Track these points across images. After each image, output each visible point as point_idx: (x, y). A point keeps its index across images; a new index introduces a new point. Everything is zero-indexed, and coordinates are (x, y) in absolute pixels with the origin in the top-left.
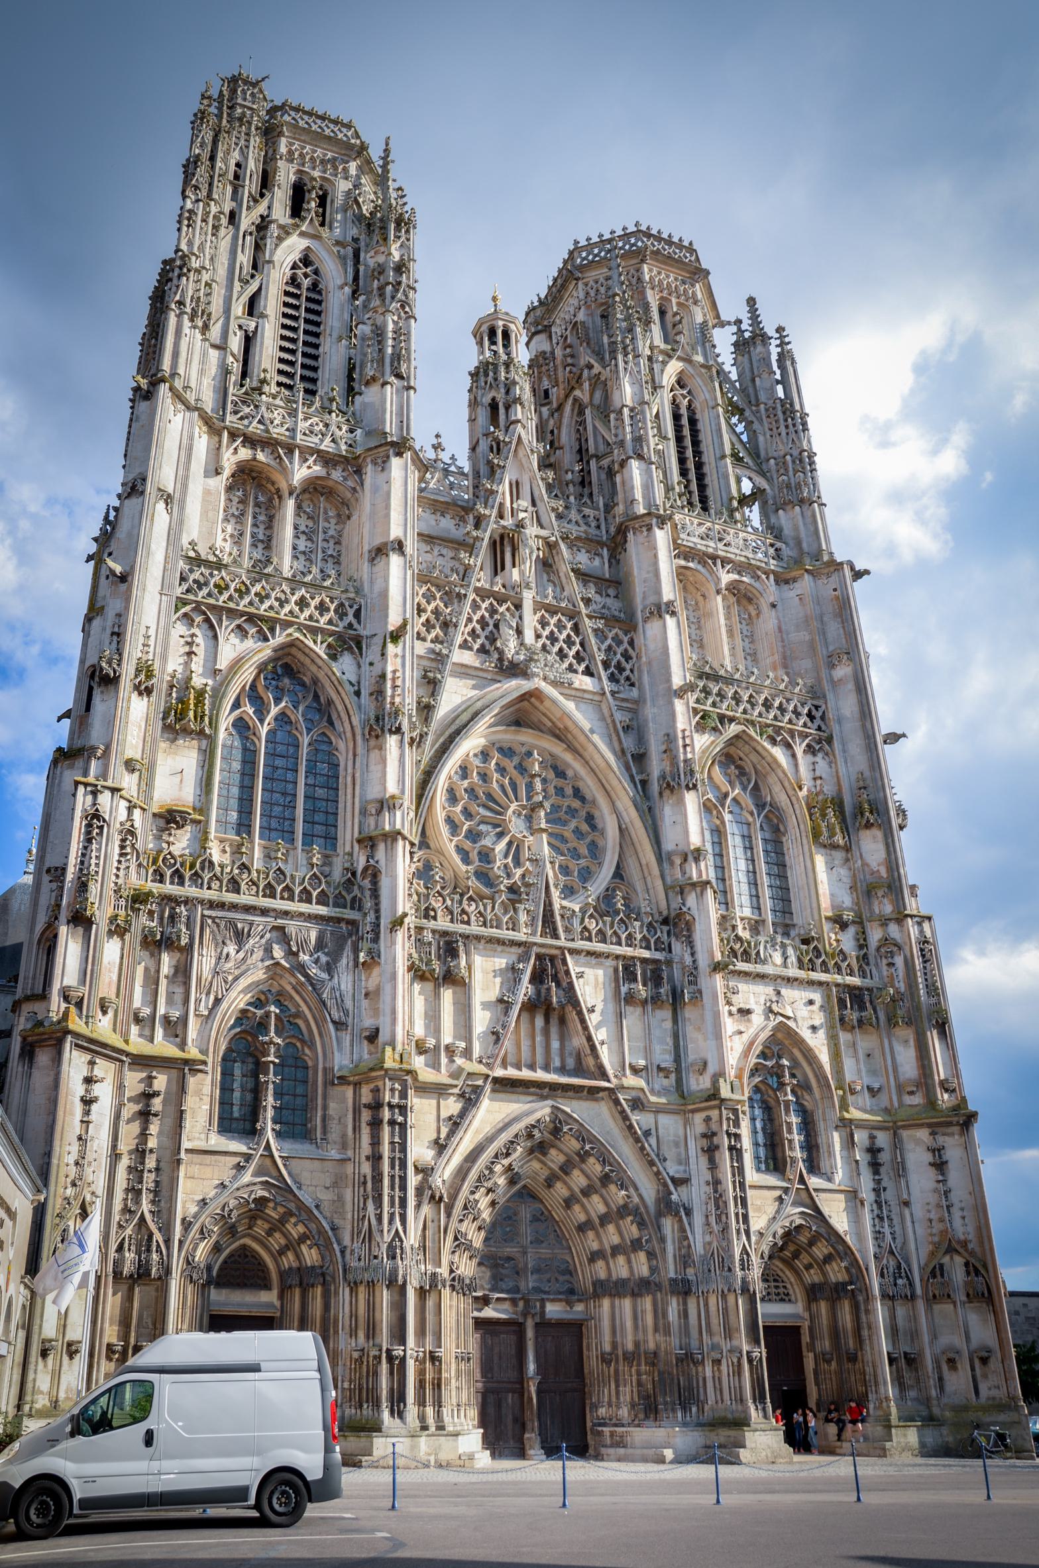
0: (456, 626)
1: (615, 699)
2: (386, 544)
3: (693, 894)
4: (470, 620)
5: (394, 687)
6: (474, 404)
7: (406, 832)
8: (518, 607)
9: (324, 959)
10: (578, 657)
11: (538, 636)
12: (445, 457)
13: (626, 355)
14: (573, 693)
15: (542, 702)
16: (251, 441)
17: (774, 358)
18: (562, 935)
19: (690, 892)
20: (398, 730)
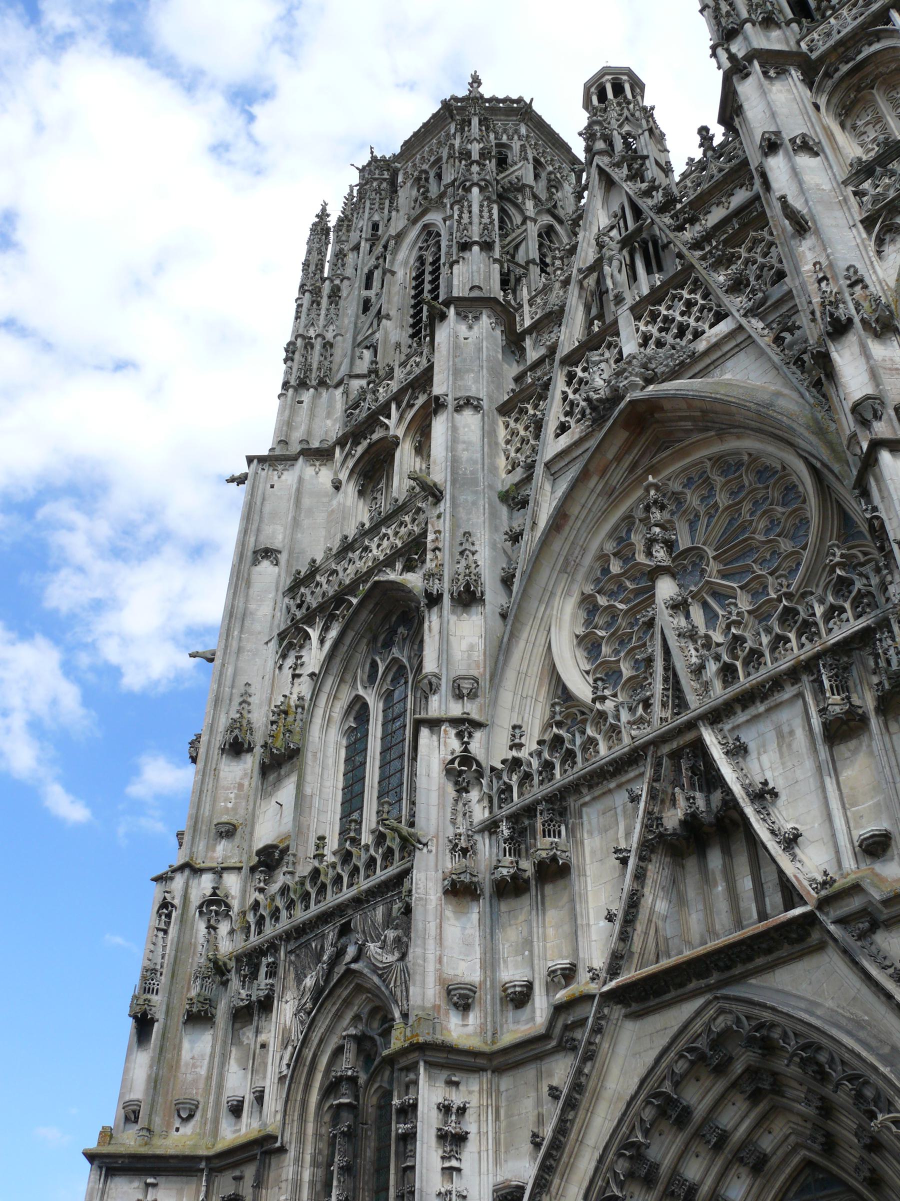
4: (565, 397)
9: (391, 934)
14: (708, 361)
15: (661, 409)
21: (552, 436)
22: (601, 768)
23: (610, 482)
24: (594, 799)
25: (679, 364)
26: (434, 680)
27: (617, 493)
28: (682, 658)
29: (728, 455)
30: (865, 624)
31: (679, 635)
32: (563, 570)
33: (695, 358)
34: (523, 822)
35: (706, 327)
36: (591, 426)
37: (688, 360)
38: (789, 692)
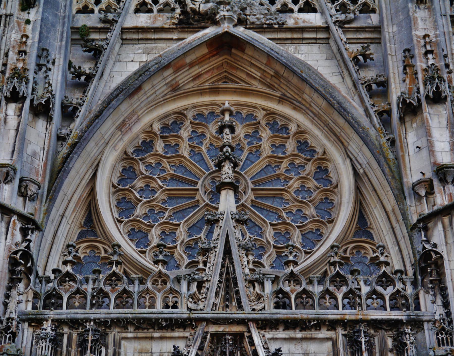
1: (345, 31)
3: (440, 226)
14: (289, 36)
15: (243, 51)
19: (436, 225)
21: (133, 8)
22: (157, 320)
23: (177, 79)
24: (135, 338)
25: (268, 24)
26: (12, 173)
27: (182, 92)
28: (241, 265)
29: (280, 115)
30: (400, 318)
31: (239, 246)
32: (120, 128)
33: (282, 28)
34: (63, 329)
35: (296, 8)
36: (176, 24)
37: (276, 26)
38: (324, 333)
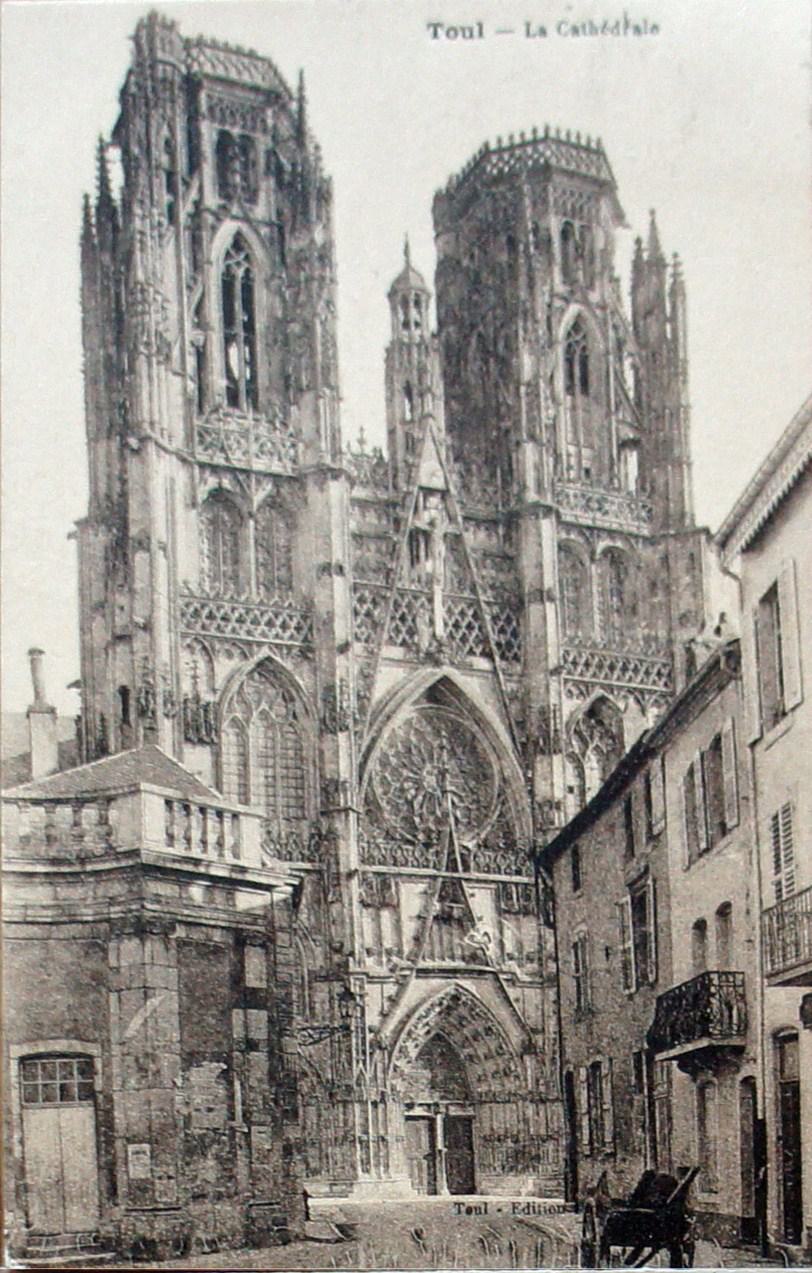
0: (383, 625)
2: (329, 564)
5: (342, 693)
6: (389, 380)
7: (354, 808)
8: (431, 600)
10: (478, 641)
11: (446, 625)
12: (368, 450)
13: (525, 321)
16: (215, 469)
17: (667, 287)
18: (460, 868)
20: (347, 728)
